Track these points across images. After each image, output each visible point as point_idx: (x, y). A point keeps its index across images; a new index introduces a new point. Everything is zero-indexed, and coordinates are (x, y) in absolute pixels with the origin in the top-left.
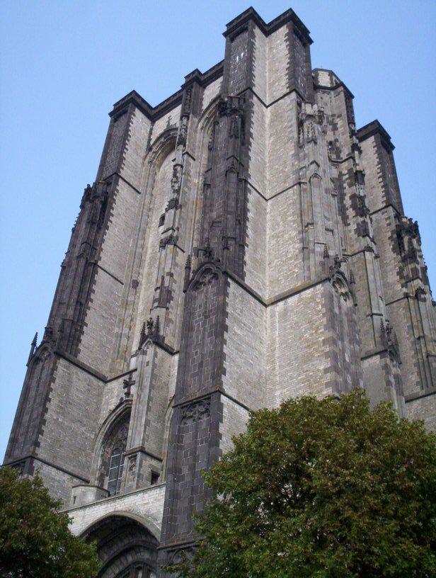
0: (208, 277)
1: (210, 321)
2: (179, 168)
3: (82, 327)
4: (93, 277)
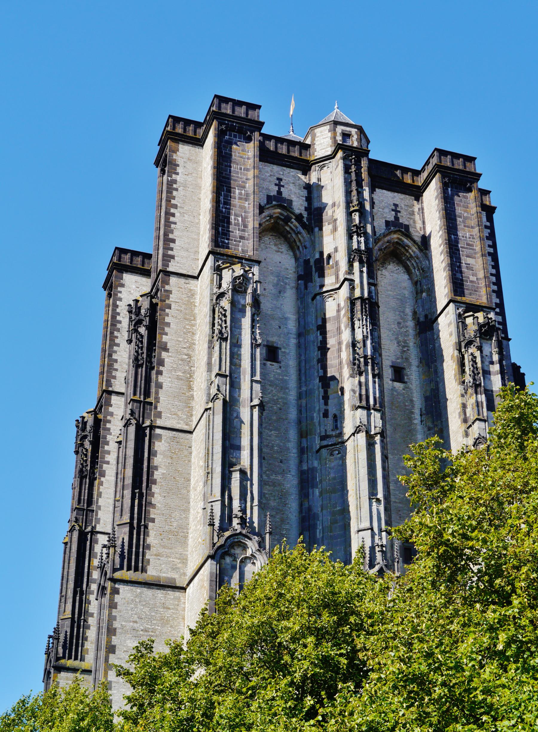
3: (85, 621)
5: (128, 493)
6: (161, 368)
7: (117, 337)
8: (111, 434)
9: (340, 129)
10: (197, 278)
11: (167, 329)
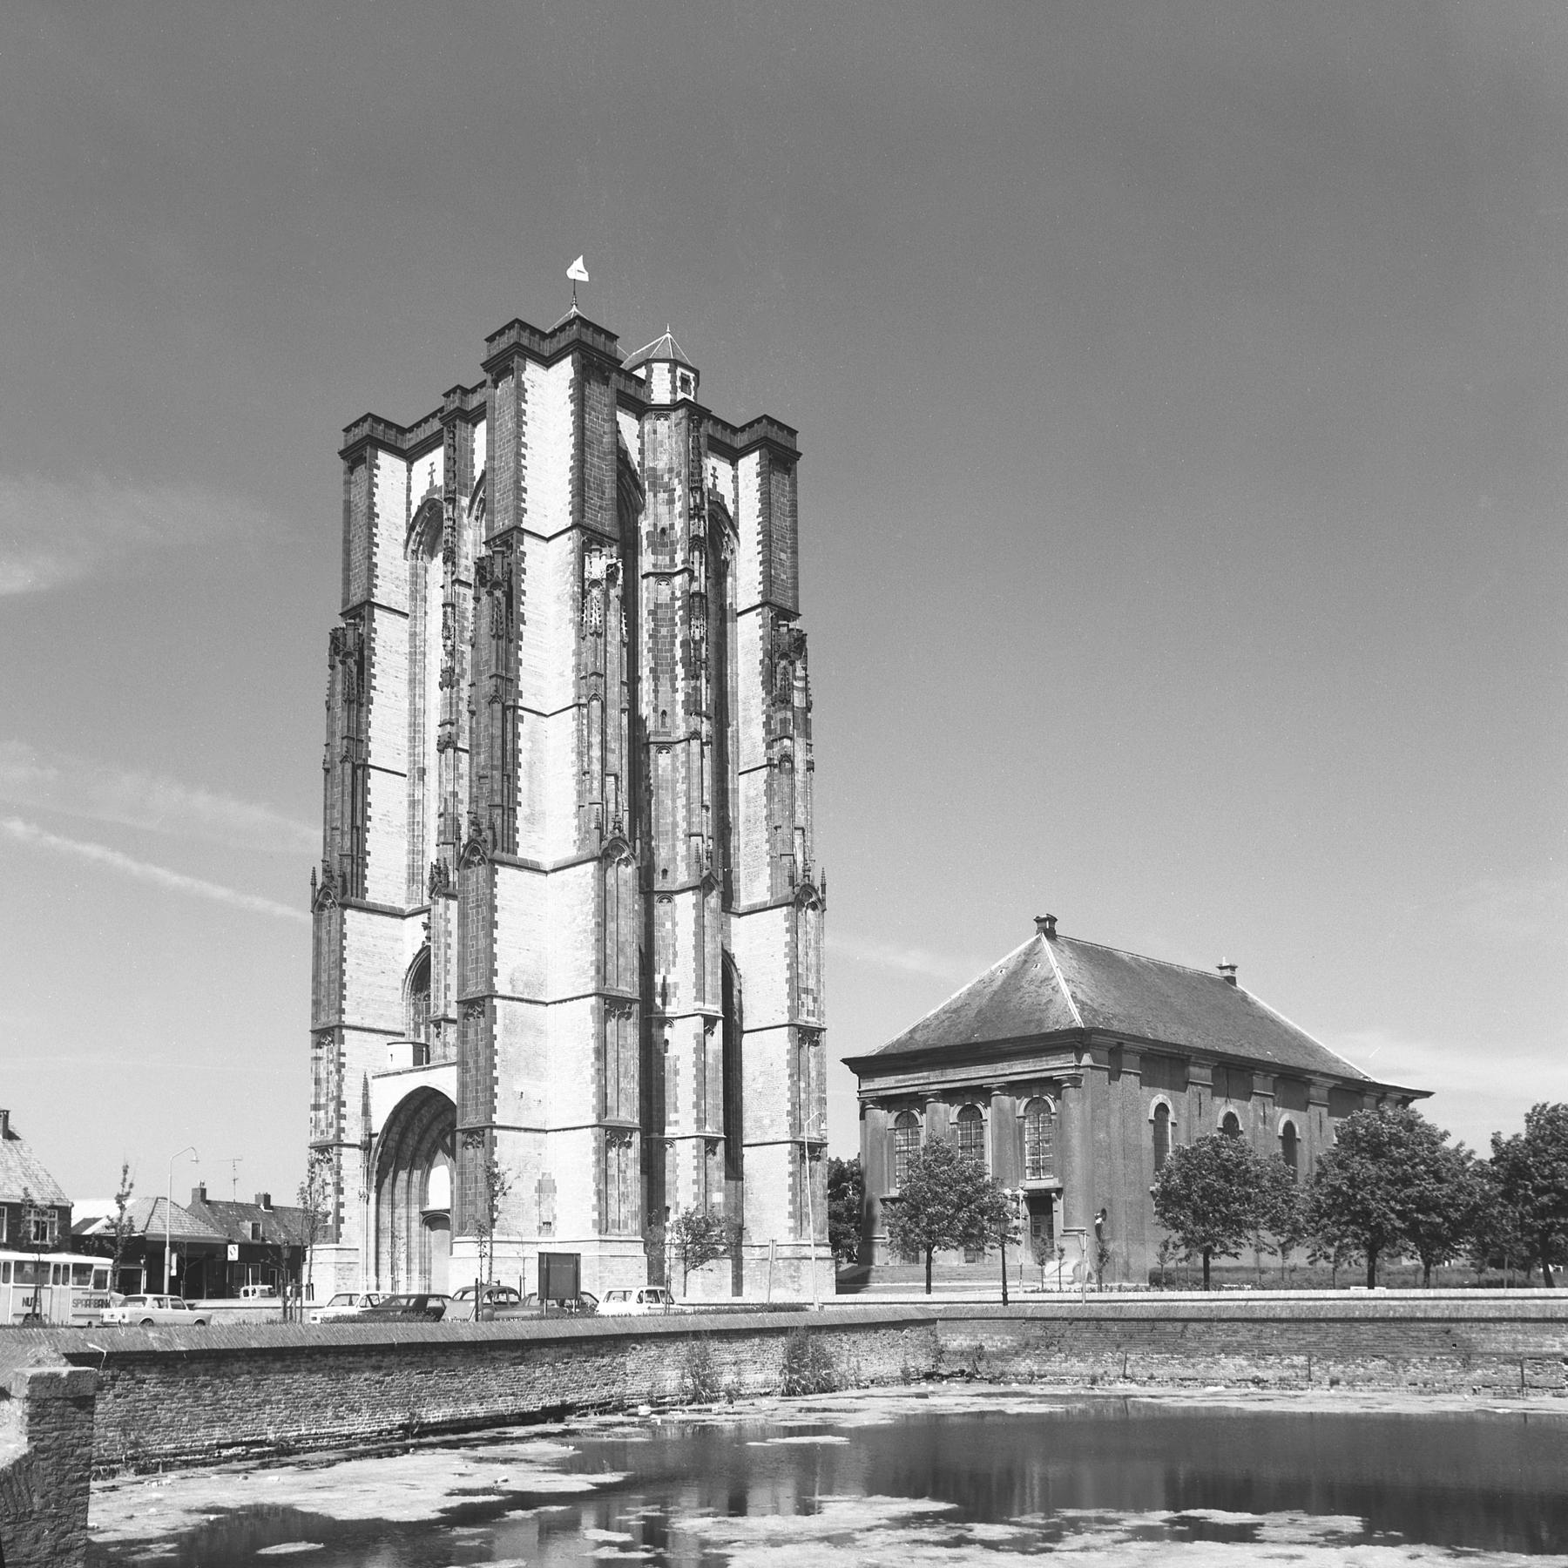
0: (476, 859)
1: (482, 913)
2: (449, 609)
3: (364, 859)
4: (364, 783)
5: (497, 774)
6: (520, 643)
7: (375, 535)
8: (375, 655)
9: (679, 371)
10: (548, 540)
11: (523, 598)
